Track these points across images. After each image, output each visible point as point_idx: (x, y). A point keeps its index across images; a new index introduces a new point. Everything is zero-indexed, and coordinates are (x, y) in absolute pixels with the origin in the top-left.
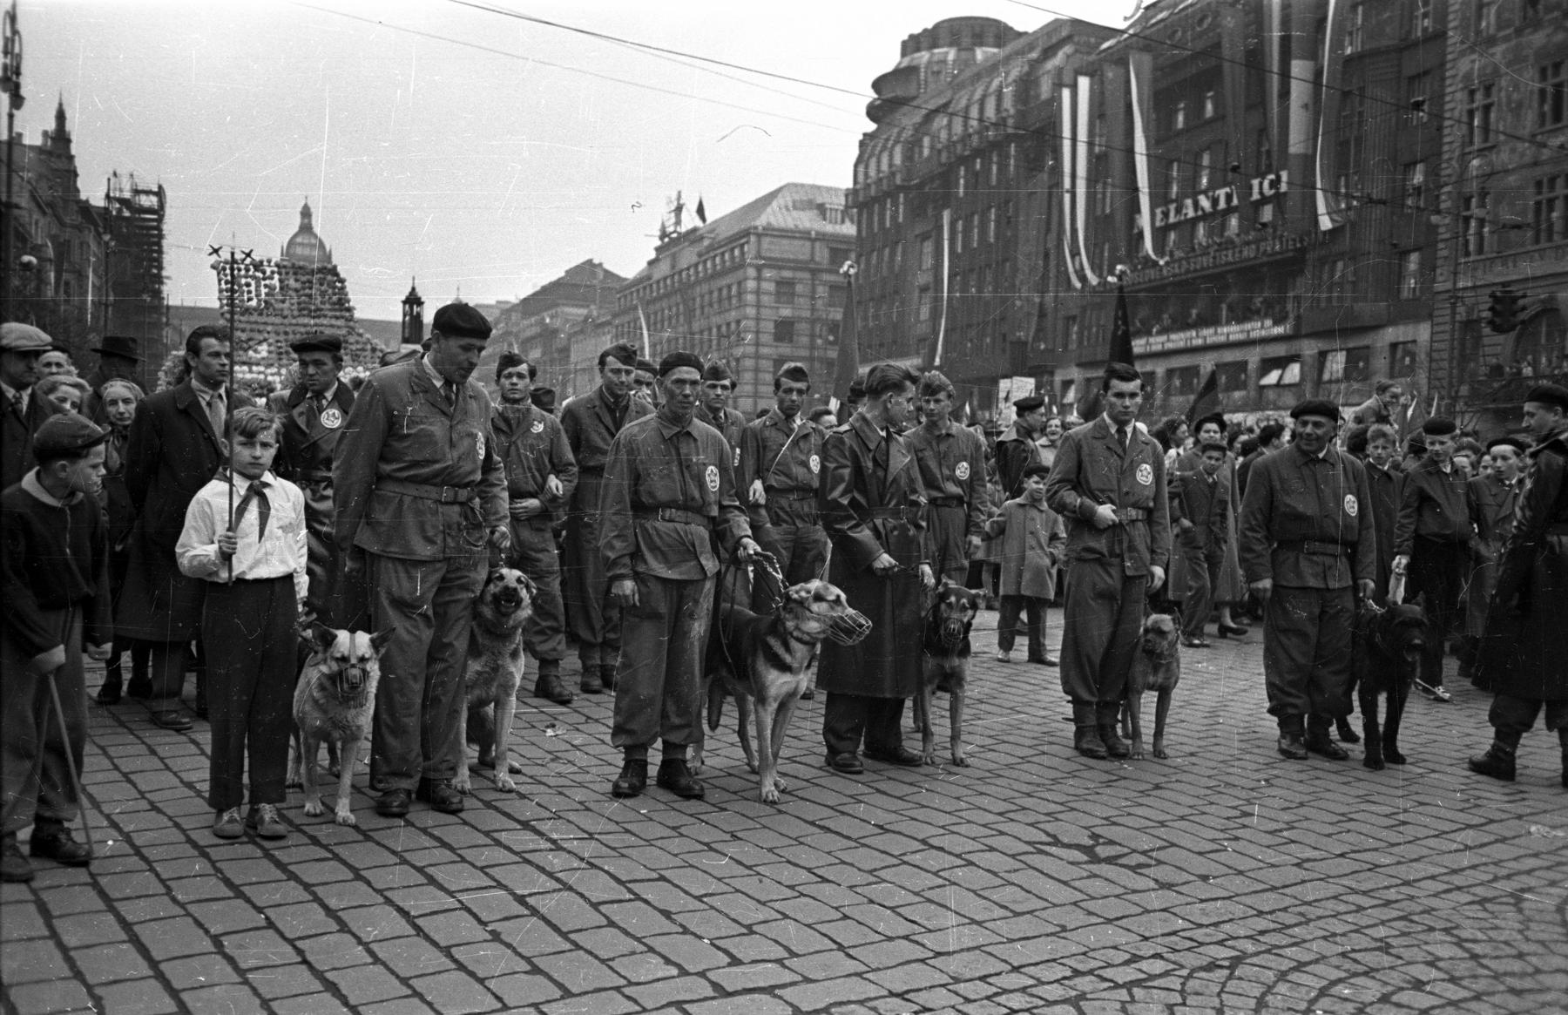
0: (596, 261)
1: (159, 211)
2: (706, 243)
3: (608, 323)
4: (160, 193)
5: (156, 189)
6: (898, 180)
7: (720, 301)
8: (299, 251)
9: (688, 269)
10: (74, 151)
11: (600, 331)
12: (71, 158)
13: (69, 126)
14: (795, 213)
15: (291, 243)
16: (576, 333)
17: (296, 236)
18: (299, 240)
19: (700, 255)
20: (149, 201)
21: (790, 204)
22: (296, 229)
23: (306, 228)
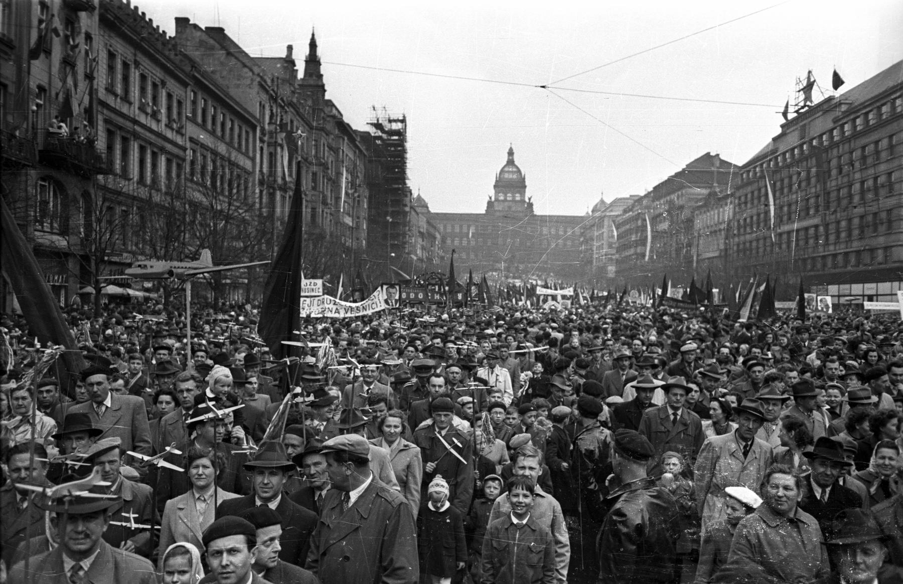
0: (713, 154)
1: (401, 134)
2: (844, 108)
4: (403, 121)
5: (401, 118)
7: (864, 158)
8: (506, 176)
9: (821, 136)
10: (322, 72)
12: (320, 76)
13: (320, 52)
15: (502, 171)
16: (699, 207)
18: (506, 169)
19: (835, 121)
20: (396, 126)
22: (505, 163)
23: (511, 162)
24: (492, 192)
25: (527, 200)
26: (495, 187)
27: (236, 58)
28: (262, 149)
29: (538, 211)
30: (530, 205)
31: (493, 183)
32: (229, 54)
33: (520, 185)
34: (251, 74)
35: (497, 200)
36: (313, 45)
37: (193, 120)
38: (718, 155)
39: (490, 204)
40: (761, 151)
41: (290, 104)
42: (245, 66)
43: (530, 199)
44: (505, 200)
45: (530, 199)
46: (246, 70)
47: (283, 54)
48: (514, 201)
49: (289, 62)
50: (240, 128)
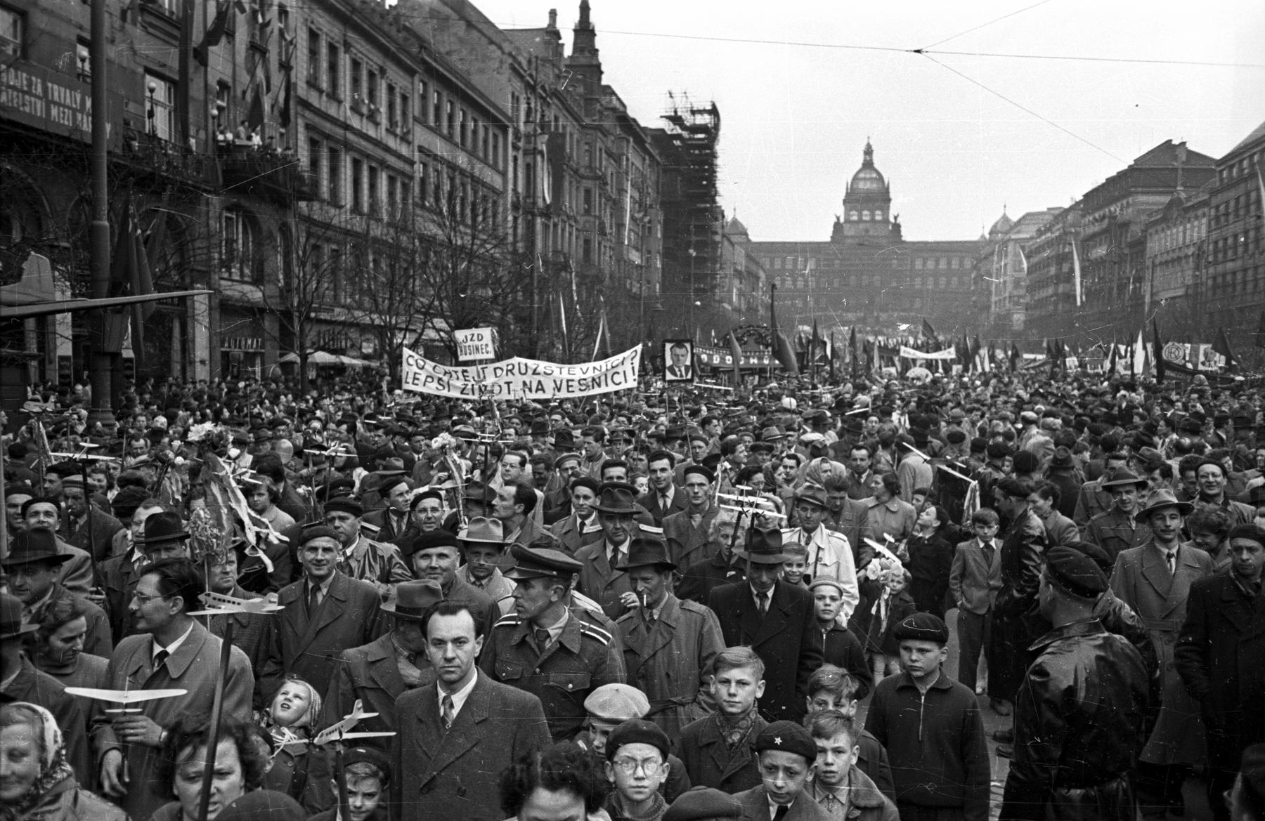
0: (1176, 142)
3: (1204, 204)
4: (714, 112)
5: (709, 107)
8: (861, 185)
10: (597, 46)
11: (1192, 214)
12: (595, 52)
13: (594, 18)
15: (855, 178)
16: (1156, 223)
18: (862, 175)
22: (859, 166)
23: (868, 165)
24: (841, 211)
26: (845, 202)
27: (480, 31)
28: (515, 159)
29: (908, 235)
30: (897, 227)
31: (842, 195)
32: (470, 25)
33: (882, 197)
34: (499, 53)
35: (847, 221)
37: (422, 120)
38: (1183, 144)
39: (838, 226)
40: (1251, 136)
41: (555, 94)
42: (492, 42)
43: (896, 218)
44: (860, 221)
45: (896, 218)
46: (493, 47)
47: (544, 23)
49: (552, 33)
50: (486, 129)
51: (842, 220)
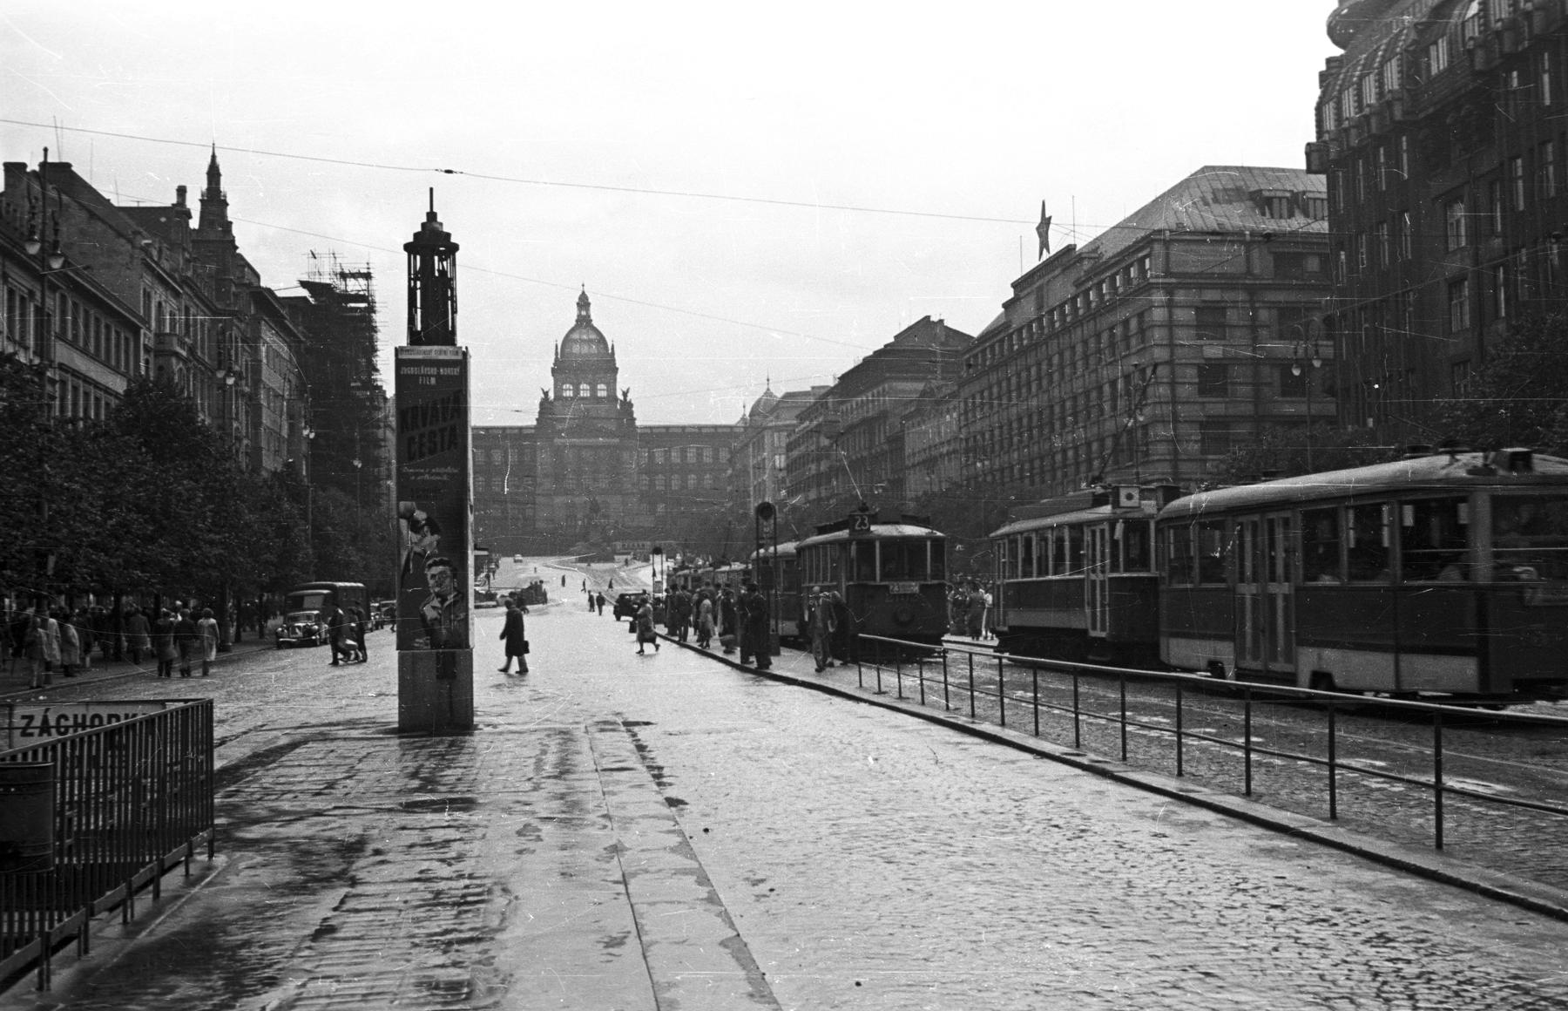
0: (934, 319)
2: (1087, 265)
5: (364, 271)
6: (1398, 113)
7: (1112, 345)
8: (576, 349)
9: (1062, 306)
11: (944, 408)
13: (225, 185)
14: (1217, 209)
15: (567, 339)
17: (572, 331)
19: (1078, 284)
20: (354, 286)
21: (1209, 197)
22: (573, 323)
23: (584, 322)
24: (549, 383)
25: (620, 397)
26: (553, 371)
27: (104, 222)
28: (147, 362)
30: (627, 406)
32: (92, 215)
34: (129, 247)
35: (558, 397)
36: (214, 173)
37: (61, 337)
38: (941, 321)
39: (545, 405)
40: (993, 323)
41: (185, 282)
42: (120, 235)
43: (625, 394)
45: (625, 394)
46: (122, 241)
47: (170, 199)
48: (594, 398)
49: (179, 211)
50: (118, 333)
51: (551, 396)
